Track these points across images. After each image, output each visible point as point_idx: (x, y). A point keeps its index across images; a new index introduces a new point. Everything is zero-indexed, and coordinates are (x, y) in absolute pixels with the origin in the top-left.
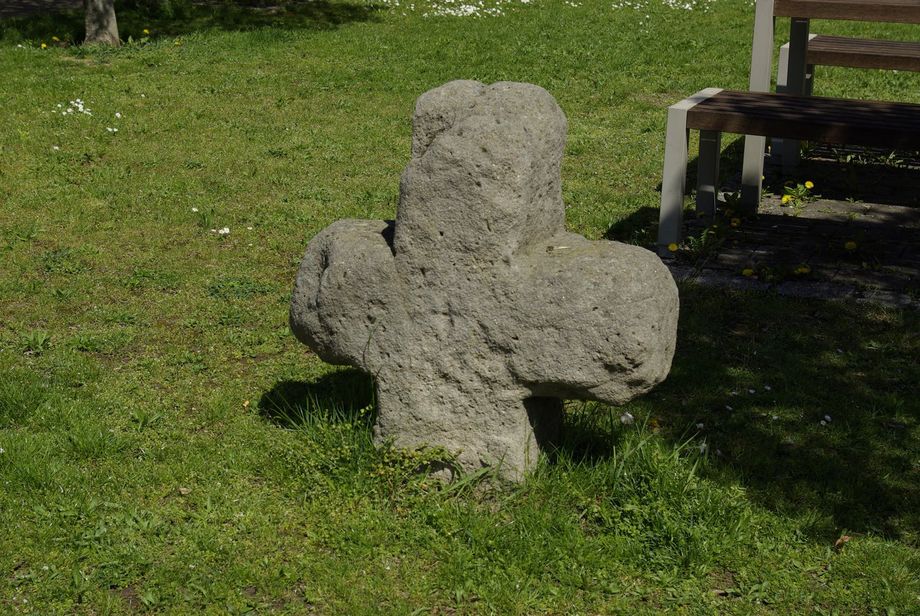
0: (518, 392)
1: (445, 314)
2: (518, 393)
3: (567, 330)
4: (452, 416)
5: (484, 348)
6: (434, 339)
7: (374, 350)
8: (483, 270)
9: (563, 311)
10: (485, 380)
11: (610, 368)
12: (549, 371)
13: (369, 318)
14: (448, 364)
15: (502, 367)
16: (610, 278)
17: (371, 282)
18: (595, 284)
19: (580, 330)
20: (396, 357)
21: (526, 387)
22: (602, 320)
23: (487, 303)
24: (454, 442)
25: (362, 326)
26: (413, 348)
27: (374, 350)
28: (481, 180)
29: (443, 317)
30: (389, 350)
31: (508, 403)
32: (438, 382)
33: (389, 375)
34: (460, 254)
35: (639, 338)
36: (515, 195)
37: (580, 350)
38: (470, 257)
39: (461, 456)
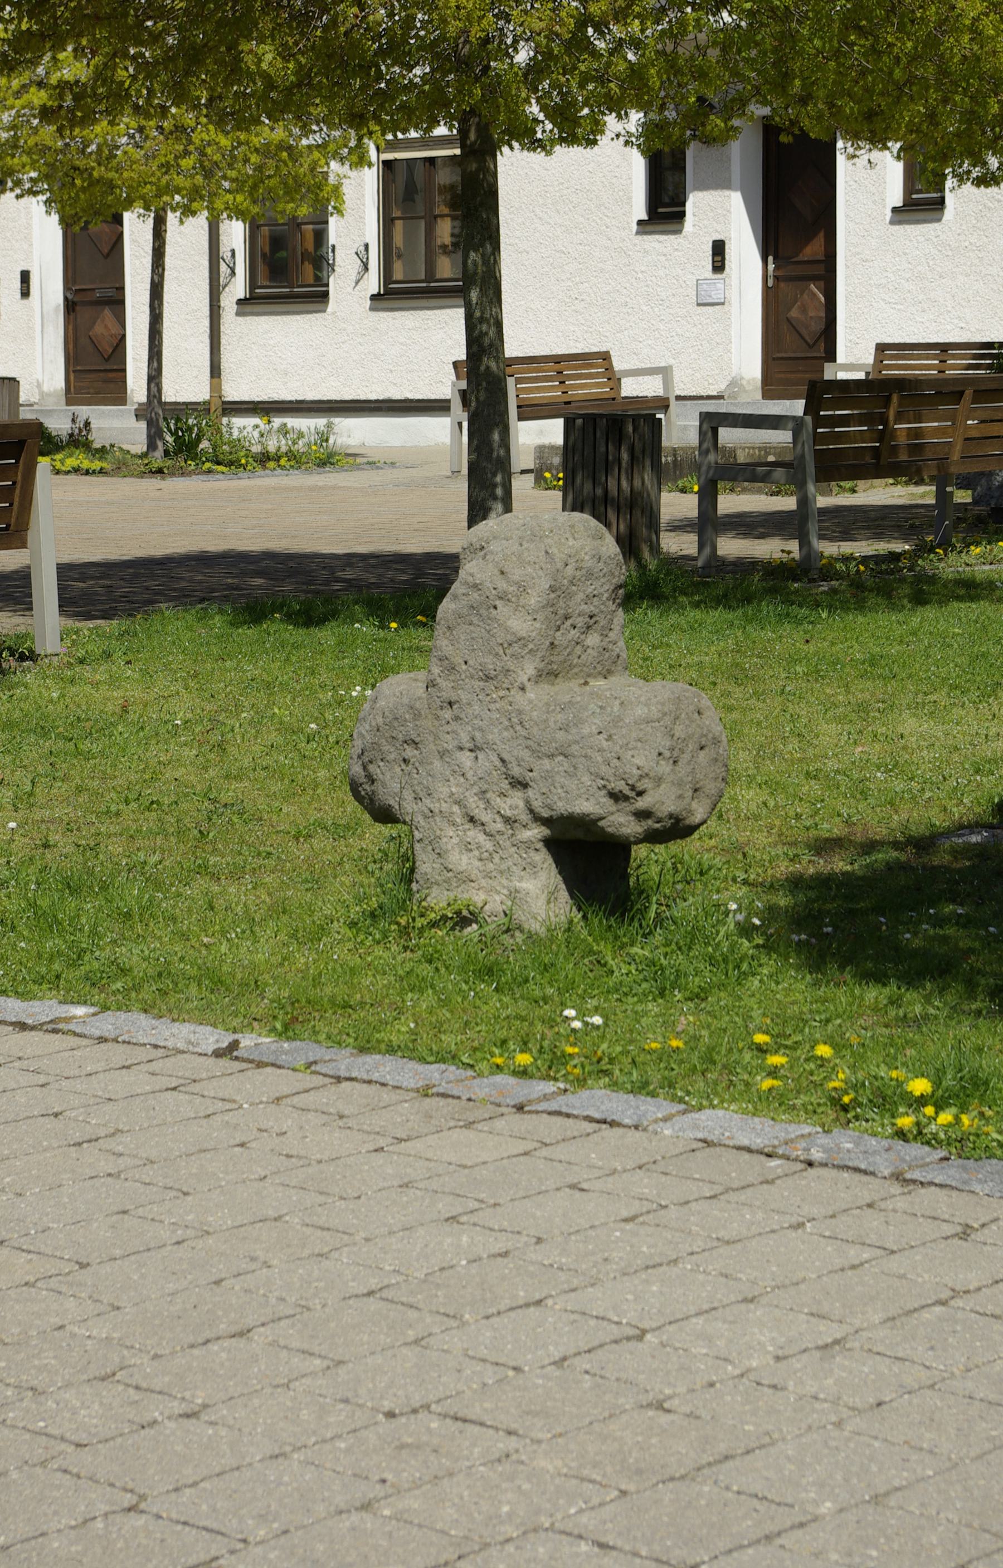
0: (536, 831)
1: (471, 750)
2: (536, 832)
3: (574, 757)
4: (479, 864)
5: (505, 785)
6: (462, 780)
7: (408, 795)
8: (501, 698)
9: (570, 737)
10: (507, 820)
11: (616, 796)
12: (560, 804)
13: (404, 760)
14: (474, 805)
15: (521, 804)
16: (617, 702)
17: (406, 720)
18: (601, 707)
19: (586, 756)
20: (427, 801)
21: (543, 824)
22: (605, 744)
23: (505, 734)
24: (480, 893)
25: (398, 770)
26: (443, 791)
27: (408, 795)
28: (498, 603)
29: (468, 754)
30: (421, 795)
31: (528, 845)
32: (467, 826)
33: (422, 823)
34: (482, 684)
35: (637, 761)
36: (530, 618)
37: (586, 780)
38: (490, 686)
39: (487, 908)
